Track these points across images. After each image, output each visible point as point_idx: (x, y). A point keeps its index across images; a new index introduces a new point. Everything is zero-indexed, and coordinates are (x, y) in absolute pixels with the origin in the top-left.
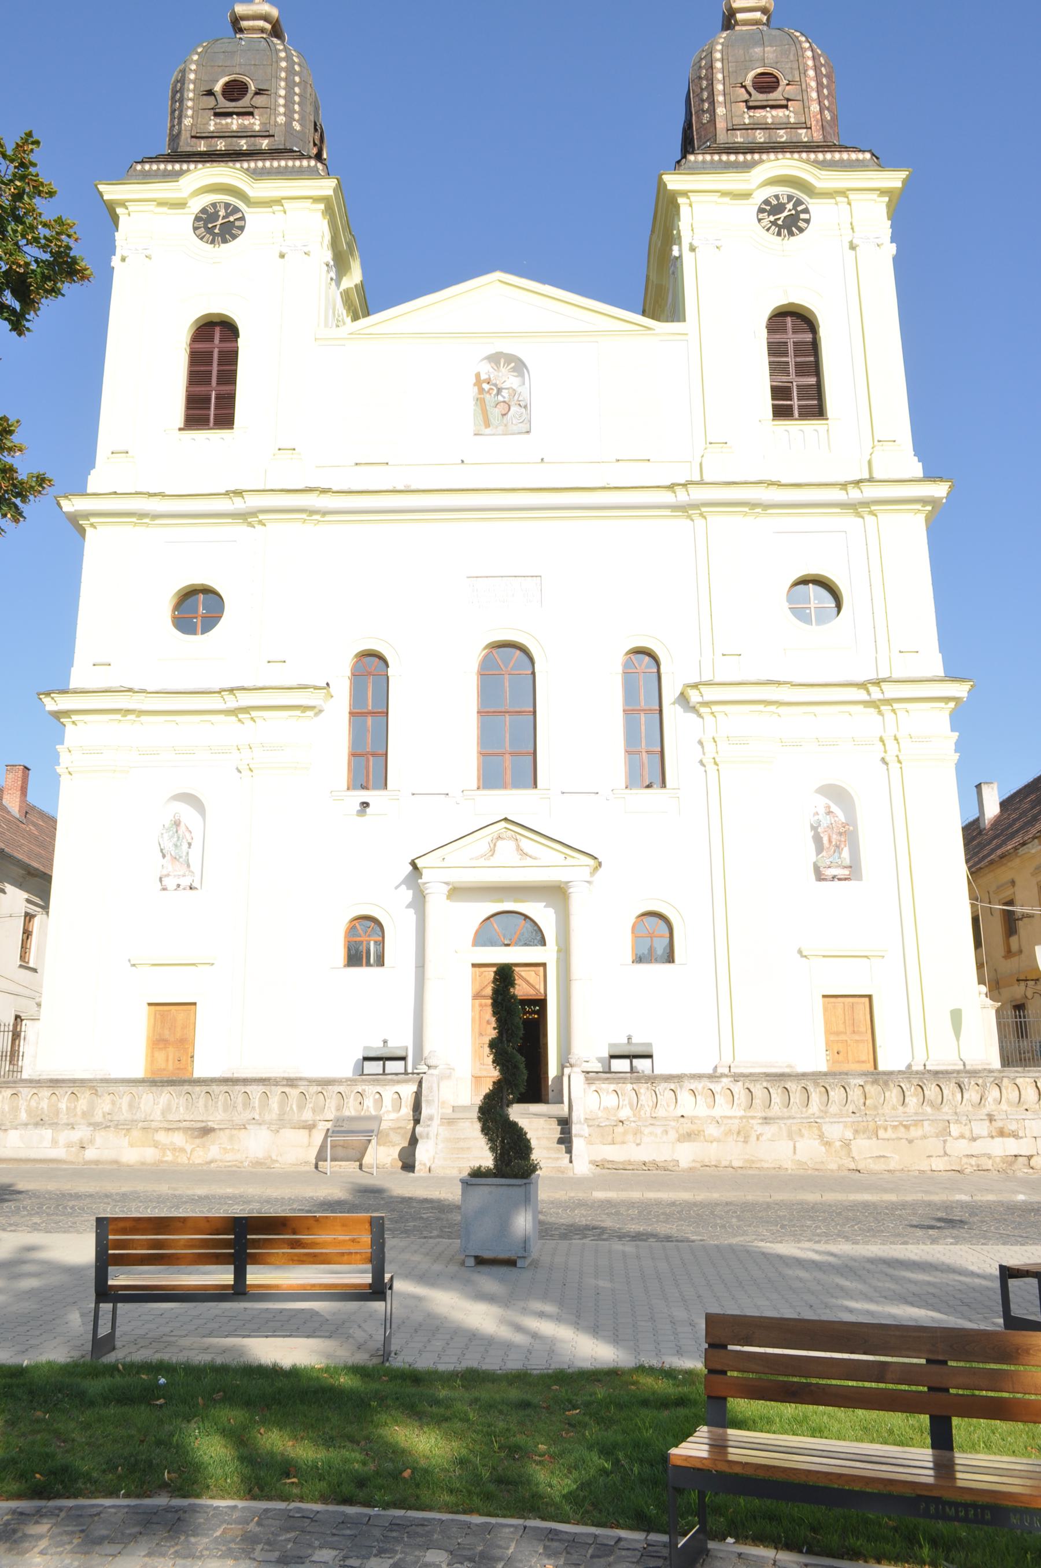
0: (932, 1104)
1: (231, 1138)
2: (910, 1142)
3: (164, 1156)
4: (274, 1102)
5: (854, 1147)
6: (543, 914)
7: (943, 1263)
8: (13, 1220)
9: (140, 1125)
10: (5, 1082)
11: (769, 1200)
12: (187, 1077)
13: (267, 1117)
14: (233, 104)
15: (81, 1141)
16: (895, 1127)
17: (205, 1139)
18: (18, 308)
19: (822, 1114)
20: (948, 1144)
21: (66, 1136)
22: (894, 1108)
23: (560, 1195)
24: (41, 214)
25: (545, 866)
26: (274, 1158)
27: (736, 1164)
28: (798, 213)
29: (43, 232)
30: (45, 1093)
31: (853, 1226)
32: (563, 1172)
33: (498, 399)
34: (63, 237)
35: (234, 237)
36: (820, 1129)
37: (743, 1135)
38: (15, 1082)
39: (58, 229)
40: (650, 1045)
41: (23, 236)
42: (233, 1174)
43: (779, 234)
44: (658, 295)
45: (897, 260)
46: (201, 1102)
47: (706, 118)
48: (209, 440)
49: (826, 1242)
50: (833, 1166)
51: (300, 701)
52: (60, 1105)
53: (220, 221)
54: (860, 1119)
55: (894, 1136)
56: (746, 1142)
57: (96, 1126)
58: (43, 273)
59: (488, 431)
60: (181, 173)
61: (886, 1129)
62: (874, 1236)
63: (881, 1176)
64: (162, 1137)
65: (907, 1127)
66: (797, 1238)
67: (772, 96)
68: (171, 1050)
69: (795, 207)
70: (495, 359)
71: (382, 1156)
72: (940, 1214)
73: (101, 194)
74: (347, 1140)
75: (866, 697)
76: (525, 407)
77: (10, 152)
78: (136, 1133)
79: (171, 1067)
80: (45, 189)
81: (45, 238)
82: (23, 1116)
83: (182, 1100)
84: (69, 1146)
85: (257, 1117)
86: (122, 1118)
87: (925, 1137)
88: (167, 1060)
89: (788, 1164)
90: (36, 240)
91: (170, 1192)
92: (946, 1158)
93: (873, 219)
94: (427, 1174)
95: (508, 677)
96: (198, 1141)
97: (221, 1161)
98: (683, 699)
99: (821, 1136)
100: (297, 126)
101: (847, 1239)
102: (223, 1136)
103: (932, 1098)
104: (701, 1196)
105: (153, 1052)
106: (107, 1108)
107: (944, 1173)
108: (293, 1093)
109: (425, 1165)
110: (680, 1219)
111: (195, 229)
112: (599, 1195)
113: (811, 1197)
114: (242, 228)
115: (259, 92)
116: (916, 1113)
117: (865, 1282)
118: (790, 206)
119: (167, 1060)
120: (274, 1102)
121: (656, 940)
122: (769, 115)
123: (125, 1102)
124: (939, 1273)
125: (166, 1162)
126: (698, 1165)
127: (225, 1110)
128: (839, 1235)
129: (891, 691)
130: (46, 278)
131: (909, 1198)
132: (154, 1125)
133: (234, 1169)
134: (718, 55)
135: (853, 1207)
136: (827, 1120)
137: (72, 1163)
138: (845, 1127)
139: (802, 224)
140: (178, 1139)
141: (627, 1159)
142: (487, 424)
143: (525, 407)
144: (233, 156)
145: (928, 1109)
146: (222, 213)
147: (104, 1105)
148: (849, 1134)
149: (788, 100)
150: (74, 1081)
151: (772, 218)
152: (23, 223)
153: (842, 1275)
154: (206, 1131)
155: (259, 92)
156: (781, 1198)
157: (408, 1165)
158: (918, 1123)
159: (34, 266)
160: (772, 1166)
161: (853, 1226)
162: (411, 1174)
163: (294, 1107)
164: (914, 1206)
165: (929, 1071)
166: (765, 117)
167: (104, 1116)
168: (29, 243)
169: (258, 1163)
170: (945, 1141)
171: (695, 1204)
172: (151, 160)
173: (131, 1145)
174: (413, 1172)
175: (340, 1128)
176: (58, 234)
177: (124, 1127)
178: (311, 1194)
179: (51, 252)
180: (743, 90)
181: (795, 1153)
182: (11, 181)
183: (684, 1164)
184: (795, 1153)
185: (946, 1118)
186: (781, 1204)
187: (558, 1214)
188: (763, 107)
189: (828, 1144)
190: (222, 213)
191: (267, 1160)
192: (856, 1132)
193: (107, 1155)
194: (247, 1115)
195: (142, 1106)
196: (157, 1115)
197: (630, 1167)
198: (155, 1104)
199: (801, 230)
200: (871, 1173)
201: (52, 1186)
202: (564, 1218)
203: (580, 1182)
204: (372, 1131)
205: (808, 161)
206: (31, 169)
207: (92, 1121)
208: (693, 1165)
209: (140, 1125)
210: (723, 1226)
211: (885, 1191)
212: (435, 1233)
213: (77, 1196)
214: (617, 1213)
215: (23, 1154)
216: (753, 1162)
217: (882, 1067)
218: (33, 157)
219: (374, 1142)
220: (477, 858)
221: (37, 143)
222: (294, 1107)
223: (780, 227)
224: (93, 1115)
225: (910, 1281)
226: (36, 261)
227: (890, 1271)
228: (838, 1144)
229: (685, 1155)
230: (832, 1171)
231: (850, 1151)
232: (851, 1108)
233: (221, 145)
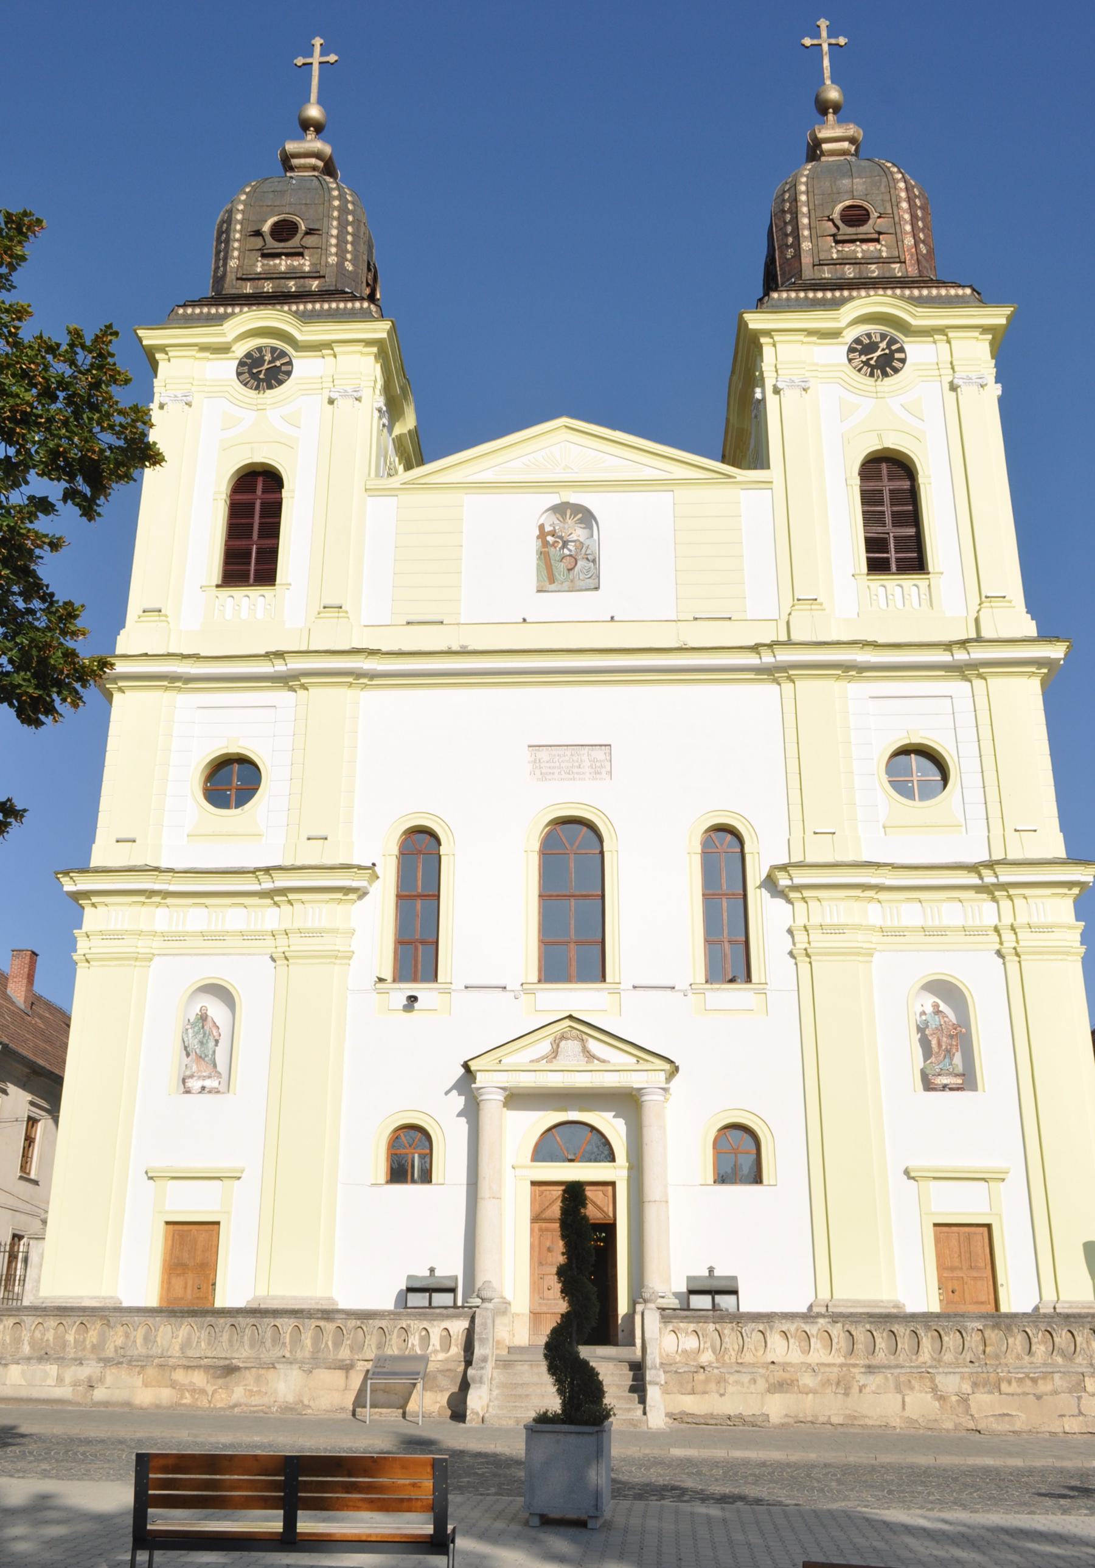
0: (1063, 1354)
1: (258, 1378)
2: (1039, 1398)
3: (182, 1397)
4: (307, 1339)
5: (972, 1403)
6: (612, 1126)
7: (1075, 1536)
8: (20, 1465)
9: (156, 1361)
10: (8, 1310)
11: (873, 1462)
12: (208, 1307)
13: (299, 1355)
14: (282, 245)
15: (90, 1379)
16: (1020, 1380)
17: (228, 1379)
18: (89, 494)
19: (934, 1363)
20: (1083, 1401)
21: (72, 1373)
22: (1019, 1357)
23: (634, 1451)
24: (117, 402)
25: (616, 1071)
26: (306, 1402)
27: (835, 1420)
28: (892, 352)
29: (118, 419)
30: (52, 1323)
31: (971, 1493)
32: (635, 1426)
33: (566, 554)
34: (139, 424)
35: (280, 382)
36: (932, 1380)
37: (844, 1385)
38: (18, 1309)
39: (133, 416)
40: (735, 1278)
41: (98, 424)
42: (258, 1420)
43: (872, 375)
44: (739, 439)
45: (1001, 400)
46: (225, 1337)
47: (790, 253)
48: (249, 600)
49: (940, 1510)
50: (949, 1425)
51: (344, 883)
52: (67, 1337)
53: (266, 366)
54: (980, 1370)
55: (1019, 1391)
56: (846, 1394)
57: (106, 1362)
58: (116, 459)
59: (552, 587)
60: (225, 317)
61: (1010, 1383)
62: (996, 1504)
63: (1004, 1438)
64: (179, 1376)
65: (1034, 1381)
66: (906, 1504)
67: (862, 229)
68: (190, 1276)
69: (889, 346)
70: (560, 509)
71: (429, 1403)
72: (1073, 1483)
73: (140, 340)
74: (390, 1382)
75: (977, 881)
76: (594, 561)
77: (88, 343)
78: (151, 1371)
79: (189, 1296)
80: (122, 377)
81: (121, 425)
82: (26, 1349)
83: (204, 1334)
84: (76, 1384)
85: (288, 1355)
86: (136, 1353)
87: (1055, 1392)
88: (185, 1288)
89: (896, 1422)
90: (111, 427)
91: (190, 1439)
92: (1081, 1418)
93: (976, 356)
94: (479, 1425)
95: (573, 855)
96: (221, 1381)
97: (246, 1405)
98: (770, 883)
99: (934, 1389)
100: (349, 267)
101: (964, 1507)
102: (249, 1376)
103: (1063, 1346)
104: (795, 1457)
105: (169, 1278)
106: (120, 1341)
107: (1079, 1437)
108: (329, 1327)
109: (477, 1414)
110: (771, 1481)
111: (239, 374)
112: (678, 1452)
113: (923, 1460)
114: (289, 374)
115: (309, 232)
116: (1045, 1364)
117: (984, 1553)
118: (883, 345)
119: (185, 1288)
120: (307, 1339)
121: (739, 1156)
122: (859, 249)
123: (140, 1334)
124: (1070, 1546)
125: (184, 1405)
126: (791, 1421)
127: (252, 1346)
128: (955, 1503)
129: (1006, 876)
130: (119, 464)
131: (1038, 1463)
132: (172, 1361)
133: (261, 1414)
134: (803, 188)
135: (973, 1472)
136: (941, 1370)
137: (78, 1404)
138: (962, 1378)
139: (896, 364)
140: (198, 1378)
141: (709, 1411)
142: (552, 579)
143: (594, 561)
144: (279, 298)
145: (1060, 1360)
146: (268, 358)
147: (116, 1338)
148: (966, 1388)
149: (880, 233)
150: (84, 1310)
151: (864, 358)
152: (99, 411)
153: (958, 1546)
154: (229, 1370)
155: (309, 232)
156: (888, 1460)
157: (458, 1412)
158: (1047, 1376)
159: (108, 453)
160: (878, 1423)
161: (971, 1493)
162: (462, 1425)
163: (330, 1344)
164: (1043, 1472)
165: (1059, 1315)
166: (855, 252)
167: (116, 1351)
168: (103, 430)
169: (287, 1408)
170: (1079, 1398)
171: (788, 1465)
172: (194, 304)
173: (146, 1385)
174: (464, 1421)
175: (382, 1368)
176: (133, 421)
177: (137, 1364)
178: (349, 1445)
179: (125, 439)
180: (830, 223)
181: (904, 1408)
182: (89, 371)
183: (775, 1418)
184: (904, 1408)
185: (1080, 1370)
186: (887, 1468)
187: (631, 1472)
188: (853, 241)
189: (942, 1398)
190: (268, 358)
191: (303, 1401)
192: (975, 1385)
193: (119, 1395)
194: (277, 1352)
195: (159, 1339)
196: (175, 1351)
197: (713, 1422)
198: (173, 1337)
199: (896, 371)
200: (994, 1434)
201: (58, 1430)
202: (638, 1476)
203: (655, 1437)
204: (418, 1373)
205: (902, 298)
206: (109, 359)
207: (103, 1356)
208: (786, 1420)
209: (156, 1361)
210: (822, 1490)
211: (1010, 1454)
212: (493, 1490)
213: (88, 1442)
214: (699, 1473)
215: (24, 1393)
216: (855, 1418)
217: (1004, 1308)
218: (111, 348)
219: (419, 1386)
220: (537, 1061)
221: (116, 334)
222: (330, 1344)
223: (873, 367)
224: (103, 1349)
225: (1036, 1553)
226: (110, 448)
227: (1014, 1542)
228: (954, 1398)
229: (777, 1408)
230: (947, 1430)
231: (968, 1407)
232: (969, 1356)
233: (268, 287)
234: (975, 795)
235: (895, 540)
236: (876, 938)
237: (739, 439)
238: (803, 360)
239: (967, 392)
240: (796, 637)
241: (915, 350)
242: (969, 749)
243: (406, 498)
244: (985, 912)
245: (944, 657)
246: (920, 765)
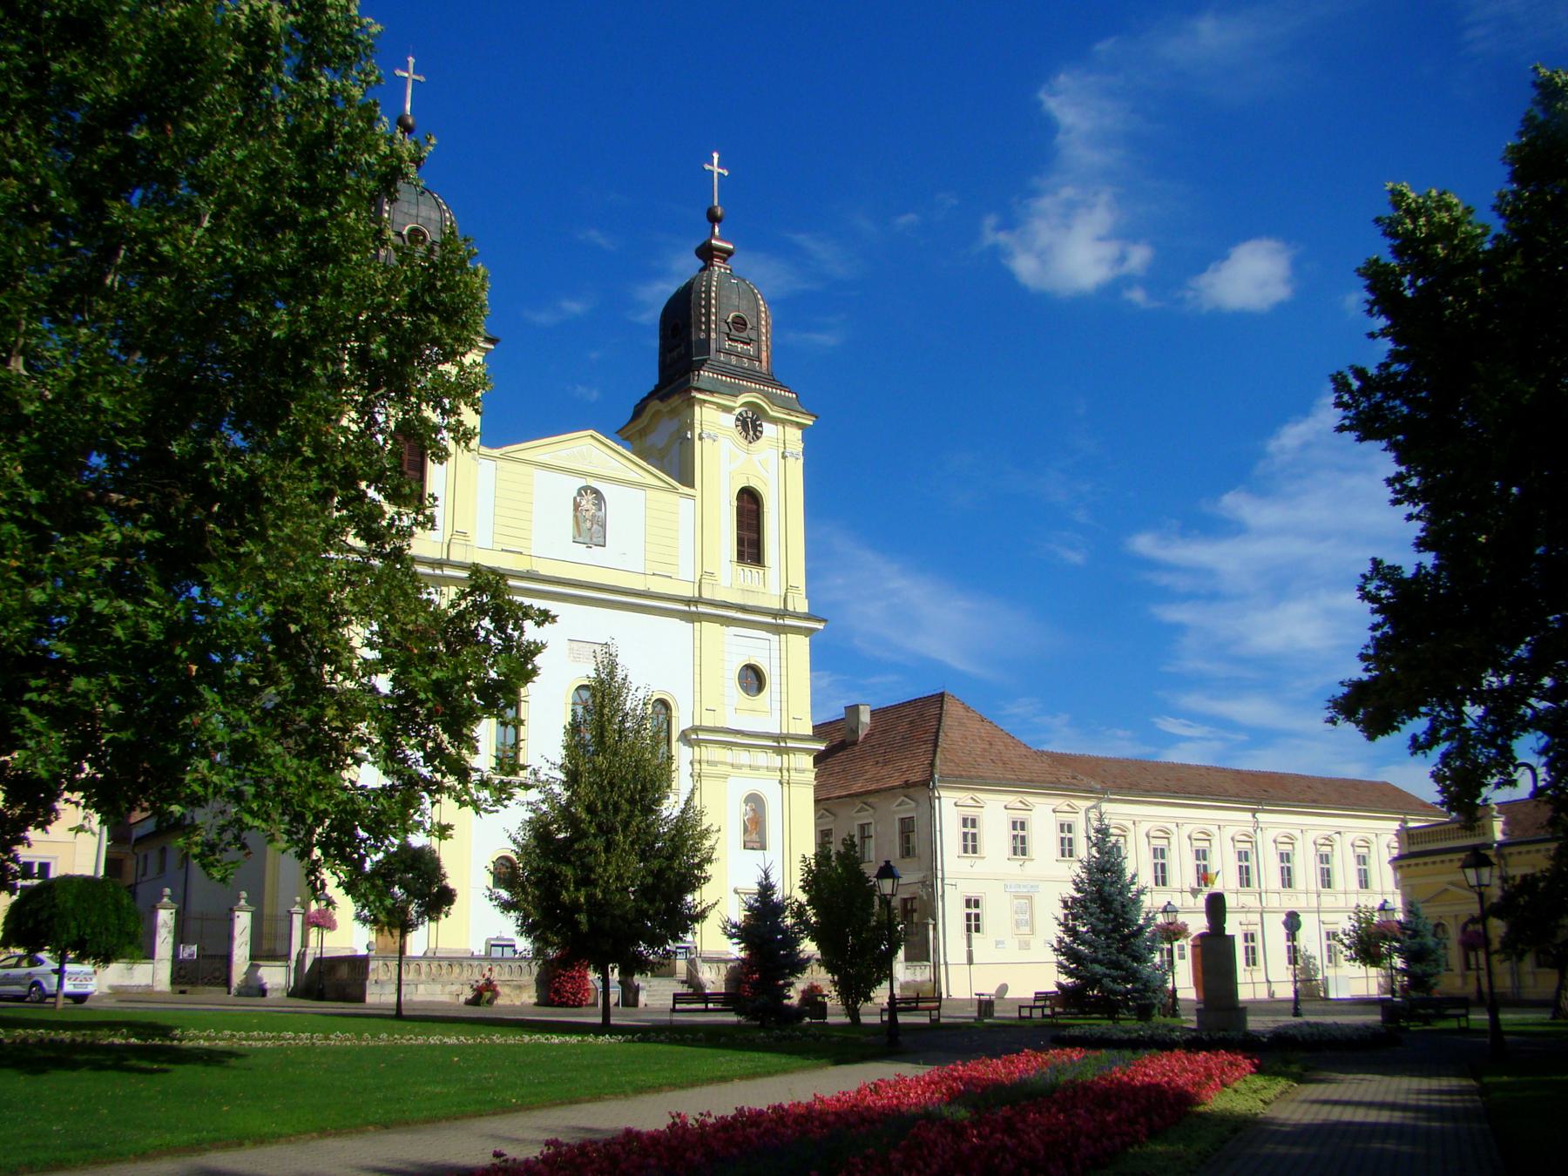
33: (589, 516)
44: (677, 464)
70: (586, 488)
98: (685, 737)
234: (776, 697)
235: (750, 548)
236: (729, 768)
237: (677, 464)
238: (713, 421)
239: (790, 460)
240: (706, 595)
241: (767, 428)
242: (775, 671)
243: (500, 463)
244: (775, 760)
245: (769, 620)
246: (753, 679)
